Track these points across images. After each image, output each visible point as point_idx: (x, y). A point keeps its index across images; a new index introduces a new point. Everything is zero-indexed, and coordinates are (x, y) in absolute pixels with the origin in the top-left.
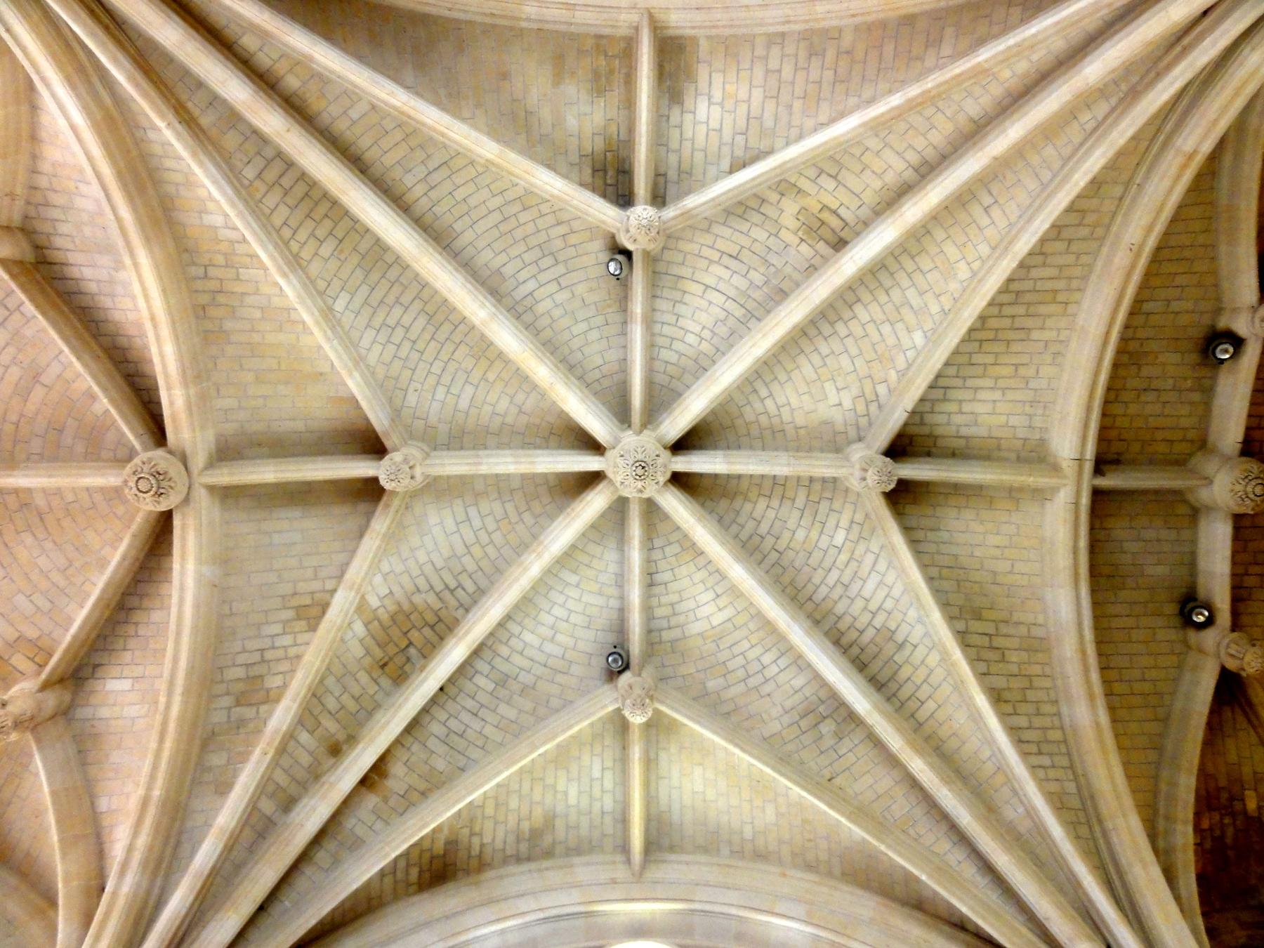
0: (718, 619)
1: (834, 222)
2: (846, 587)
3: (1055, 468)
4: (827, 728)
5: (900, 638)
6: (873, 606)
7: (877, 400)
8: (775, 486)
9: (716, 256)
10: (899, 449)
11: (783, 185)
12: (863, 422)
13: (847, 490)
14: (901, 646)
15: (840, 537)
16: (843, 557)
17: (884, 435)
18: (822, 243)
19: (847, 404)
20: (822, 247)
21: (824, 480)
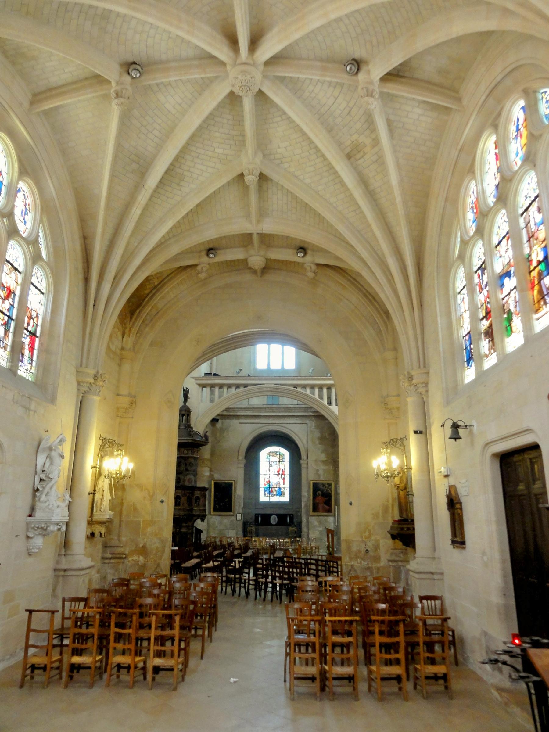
0: (167, 106)
1: (358, 156)
2: (198, 157)
3: (258, 222)
4: (135, 166)
5: (182, 183)
6: (192, 170)
7: (282, 163)
8: (239, 121)
9: (351, 104)
10: (263, 178)
11: (376, 142)
12: (272, 157)
13: (241, 151)
14: (179, 185)
15: (220, 151)
16: (210, 153)
17: (266, 172)
18: (351, 150)
19: (279, 151)
20: (348, 150)
21: (244, 141)
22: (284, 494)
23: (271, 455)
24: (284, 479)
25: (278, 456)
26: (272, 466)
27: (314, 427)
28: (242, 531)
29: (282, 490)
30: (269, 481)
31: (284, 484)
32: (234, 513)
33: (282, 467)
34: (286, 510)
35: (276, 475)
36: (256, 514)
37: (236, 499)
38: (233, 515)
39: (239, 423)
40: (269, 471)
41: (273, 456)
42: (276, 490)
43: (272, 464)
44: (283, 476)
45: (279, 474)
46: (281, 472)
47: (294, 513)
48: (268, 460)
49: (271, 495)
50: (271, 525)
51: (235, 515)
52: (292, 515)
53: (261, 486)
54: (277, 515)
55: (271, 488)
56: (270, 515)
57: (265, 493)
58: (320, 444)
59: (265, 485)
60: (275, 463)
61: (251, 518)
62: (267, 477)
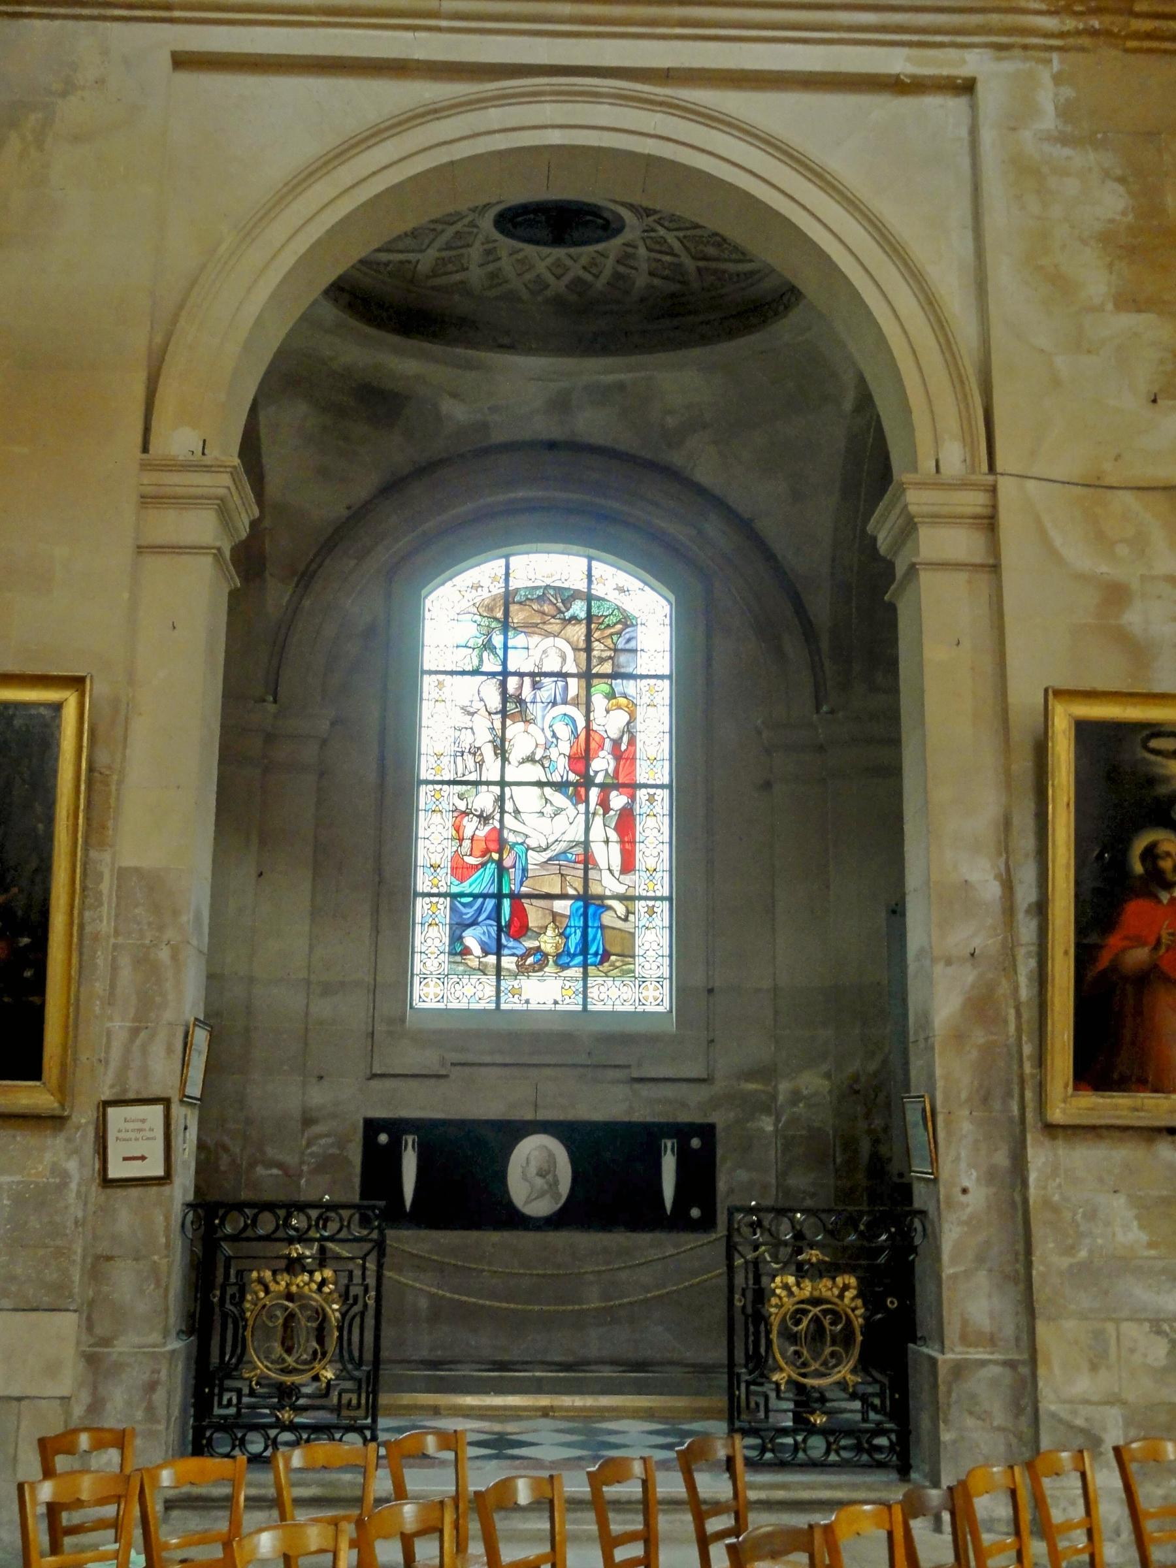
22: (628, 954)
23: (518, 616)
24: (626, 824)
25: (578, 632)
26: (523, 716)
27: (1049, 121)
28: (174, 1319)
29: (608, 919)
30: (499, 842)
31: (628, 865)
32: (64, 1090)
33: (610, 723)
34: (645, 1090)
35: (560, 786)
36: (372, 1127)
37: (103, 922)
38: (54, 1121)
39: (183, 61)
40: (501, 750)
41: (529, 628)
42: (555, 915)
43: (527, 693)
44: (618, 801)
45: (587, 781)
46: (602, 764)
47: (719, 1118)
48: (491, 664)
49: (508, 962)
50: (514, 1220)
51: (84, 1117)
52: (707, 1132)
53: (423, 882)
54: (565, 1131)
55: (516, 897)
56: (516, 1131)
57: (456, 938)
58: (1128, 301)
59: (461, 870)
60: (550, 687)
61: (325, 1164)
62: (484, 800)
